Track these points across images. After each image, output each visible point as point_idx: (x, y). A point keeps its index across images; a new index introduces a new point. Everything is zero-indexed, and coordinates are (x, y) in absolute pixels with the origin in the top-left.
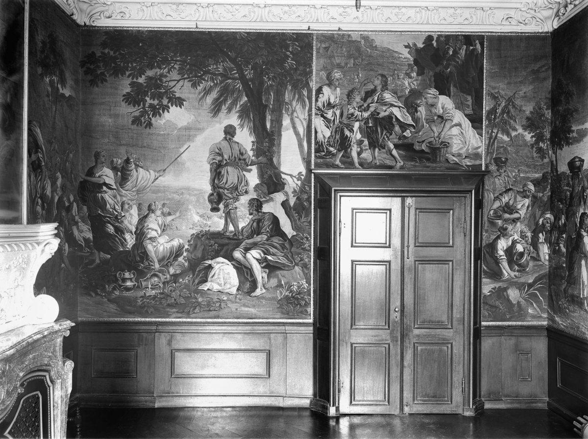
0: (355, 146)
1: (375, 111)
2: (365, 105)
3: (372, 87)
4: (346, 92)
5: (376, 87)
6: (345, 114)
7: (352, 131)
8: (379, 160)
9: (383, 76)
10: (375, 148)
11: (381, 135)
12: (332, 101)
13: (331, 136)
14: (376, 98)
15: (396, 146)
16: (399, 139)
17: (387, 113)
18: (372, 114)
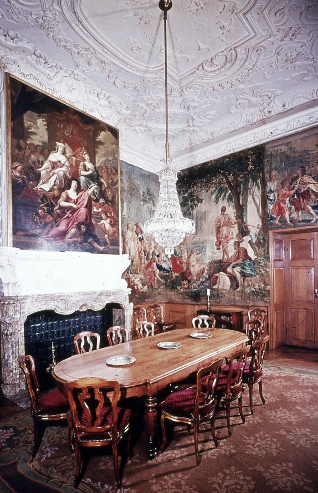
0: (288, 211)
1: (298, 189)
2: (292, 186)
3: (296, 175)
4: (280, 182)
5: (298, 175)
6: (281, 194)
7: (285, 203)
8: (302, 217)
9: (302, 167)
10: (299, 210)
11: (303, 202)
12: (272, 189)
13: (273, 208)
14: (298, 182)
15: (313, 208)
16: (315, 203)
17: (306, 189)
18: (297, 191)
